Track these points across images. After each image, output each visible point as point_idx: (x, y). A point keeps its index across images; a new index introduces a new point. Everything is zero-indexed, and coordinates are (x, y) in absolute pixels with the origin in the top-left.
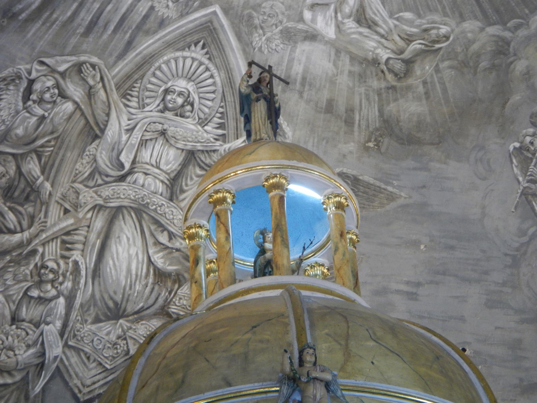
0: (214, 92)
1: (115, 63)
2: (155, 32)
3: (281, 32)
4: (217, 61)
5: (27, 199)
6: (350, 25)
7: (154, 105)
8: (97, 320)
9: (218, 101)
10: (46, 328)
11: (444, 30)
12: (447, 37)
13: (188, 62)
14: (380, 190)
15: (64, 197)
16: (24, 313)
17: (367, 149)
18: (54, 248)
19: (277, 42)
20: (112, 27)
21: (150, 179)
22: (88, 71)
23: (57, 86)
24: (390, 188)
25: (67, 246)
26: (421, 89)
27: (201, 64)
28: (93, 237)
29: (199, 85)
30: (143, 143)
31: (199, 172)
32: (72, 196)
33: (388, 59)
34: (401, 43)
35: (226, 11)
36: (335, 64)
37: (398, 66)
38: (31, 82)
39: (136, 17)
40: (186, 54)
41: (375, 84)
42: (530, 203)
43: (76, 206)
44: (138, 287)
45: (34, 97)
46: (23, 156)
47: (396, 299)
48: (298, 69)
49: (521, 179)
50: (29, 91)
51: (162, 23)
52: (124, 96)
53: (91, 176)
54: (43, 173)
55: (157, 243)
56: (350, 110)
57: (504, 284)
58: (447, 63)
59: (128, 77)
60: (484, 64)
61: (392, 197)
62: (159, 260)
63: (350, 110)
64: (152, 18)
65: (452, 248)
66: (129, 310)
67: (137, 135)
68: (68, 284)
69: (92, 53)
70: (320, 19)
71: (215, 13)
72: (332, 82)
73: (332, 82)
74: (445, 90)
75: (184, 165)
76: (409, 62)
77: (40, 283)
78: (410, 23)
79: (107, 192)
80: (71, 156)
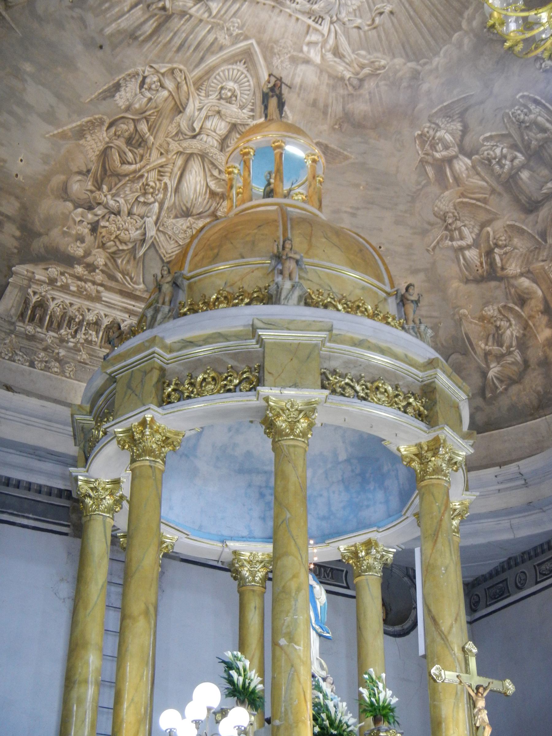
0: (249, 90)
1: (193, 69)
2: (217, 53)
3: (290, 57)
4: (252, 72)
5: (140, 145)
6: (329, 56)
7: (214, 96)
8: (176, 217)
9: (251, 95)
10: (147, 220)
11: (383, 62)
12: (384, 67)
13: (235, 72)
14: (339, 153)
15: (161, 146)
16: (135, 210)
17: (334, 129)
18: (153, 175)
19: (287, 64)
20: (192, 48)
21: (210, 139)
22: (177, 73)
23: (160, 81)
24: (345, 153)
25: (161, 174)
26: (367, 96)
27: (242, 73)
28: (176, 169)
29: (240, 85)
30: (207, 117)
31: (238, 136)
32: (165, 145)
33: (350, 78)
34: (358, 69)
35: (259, 43)
36: (319, 78)
37: (355, 82)
38: (144, 78)
39: (207, 44)
40: (234, 67)
41: (341, 91)
42: (424, 167)
43: (167, 151)
44: (200, 200)
45: (146, 86)
46: (138, 120)
49: (420, 152)
51: (221, 48)
52: (198, 89)
53: (177, 134)
54: (149, 130)
55: (212, 175)
56: (326, 106)
57: (406, 212)
58: (383, 82)
59: (200, 78)
60: (405, 84)
61: (346, 158)
62: (213, 185)
63: (326, 106)
64: (216, 44)
65: (377, 189)
66: (195, 212)
67: (204, 113)
68: (161, 196)
69: (180, 63)
70: (312, 51)
71: (252, 44)
73: (317, 88)
74: (381, 99)
75: (230, 132)
76: (361, 80)
77: (145, 194)
78: (364, 57)
79: (185, 144)
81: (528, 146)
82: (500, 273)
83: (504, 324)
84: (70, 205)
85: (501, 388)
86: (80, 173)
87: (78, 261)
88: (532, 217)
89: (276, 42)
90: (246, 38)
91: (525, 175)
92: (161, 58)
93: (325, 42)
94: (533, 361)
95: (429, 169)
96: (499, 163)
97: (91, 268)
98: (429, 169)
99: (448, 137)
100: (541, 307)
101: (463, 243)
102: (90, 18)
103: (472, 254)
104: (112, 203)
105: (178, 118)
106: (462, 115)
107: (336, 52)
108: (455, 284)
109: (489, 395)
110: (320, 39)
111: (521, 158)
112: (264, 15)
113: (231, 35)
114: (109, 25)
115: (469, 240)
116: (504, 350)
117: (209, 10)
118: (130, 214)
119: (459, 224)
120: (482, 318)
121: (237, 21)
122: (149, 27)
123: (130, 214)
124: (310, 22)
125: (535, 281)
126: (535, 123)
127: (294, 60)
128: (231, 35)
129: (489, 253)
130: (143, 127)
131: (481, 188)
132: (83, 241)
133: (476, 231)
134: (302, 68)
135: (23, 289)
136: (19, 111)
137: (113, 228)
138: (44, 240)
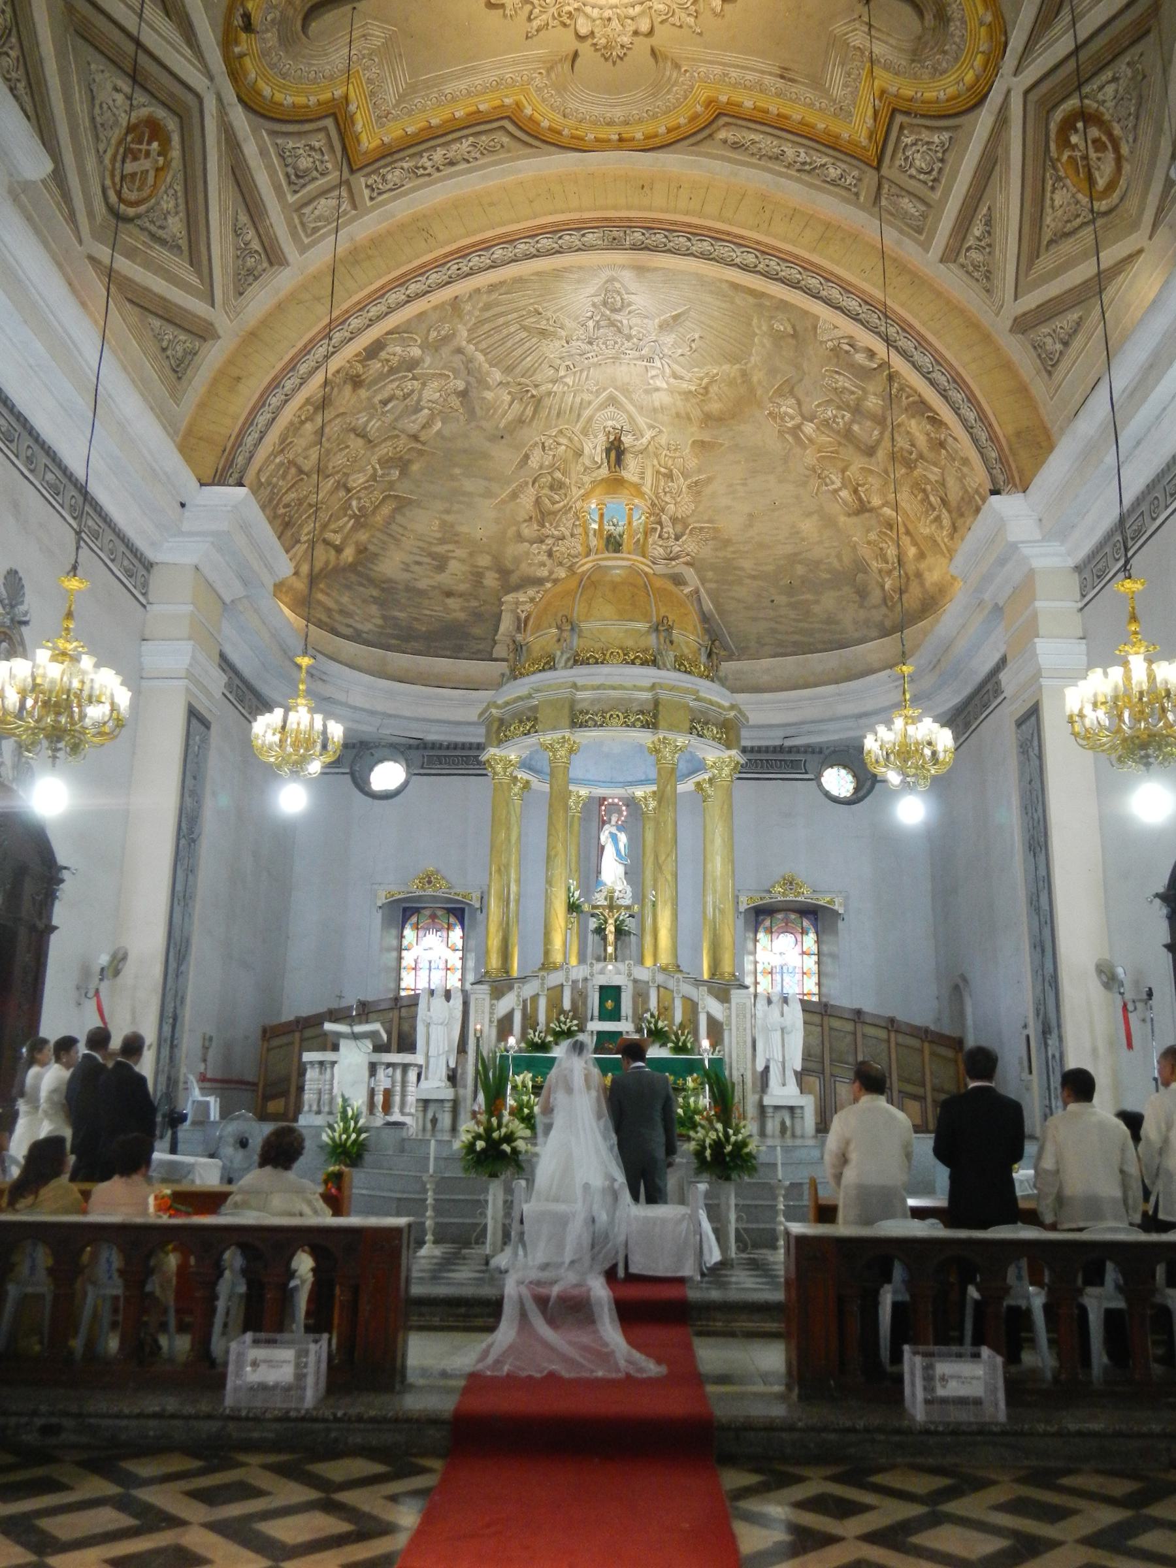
6: (672, 380)
22: (565, 432)
29: (618, 421)
37: (702, 391)
39: (577, 405)
41: (694, 401)
43: (583, 484)
47: (739, 487)
48: (657, 404)
51: (590, 403)
60: (739, 381)
61: (721, 445)
72: (675, 404)
73: (675, 404)
79: (594, 474)
81: (848, 406)
82: (868, 506)
83: (884, 545)
84: (526, 544)
86: (525, 521)
87: (547, 580)
88: (873, 460)
89: (628, 384)
90: (605, 389)
91: (856, 428)
93: (663, 372)
94: (910, 573)
95: (787, 436)
96: (834, 421)
97: (556, 581)
98: (787, 436)
99: (790, 411)
101: (834, 487)
102: (484, 424)
103: (844, 494)
104: (556, 533)
105: (581, 460)
106: (791, 392)
107: (675, 376)
108: (842, 519)
109: (890, 604)
111: (848, 416)
115: (838, 484)
117: (566, 384)
118: (572, 535)
119: (826, 472)
120: (869, 543)
122: (529, 411)
123: (572, 535)
126: (845, 388)
127: (647, 392)
129: (856, 491)
130: (558, 475)
131: (830, 443)
132: (544, 565)
133: (840, 475)
134: (656, 395)
135: (514, 611)
136: (466, 499)
137: (563, 549)
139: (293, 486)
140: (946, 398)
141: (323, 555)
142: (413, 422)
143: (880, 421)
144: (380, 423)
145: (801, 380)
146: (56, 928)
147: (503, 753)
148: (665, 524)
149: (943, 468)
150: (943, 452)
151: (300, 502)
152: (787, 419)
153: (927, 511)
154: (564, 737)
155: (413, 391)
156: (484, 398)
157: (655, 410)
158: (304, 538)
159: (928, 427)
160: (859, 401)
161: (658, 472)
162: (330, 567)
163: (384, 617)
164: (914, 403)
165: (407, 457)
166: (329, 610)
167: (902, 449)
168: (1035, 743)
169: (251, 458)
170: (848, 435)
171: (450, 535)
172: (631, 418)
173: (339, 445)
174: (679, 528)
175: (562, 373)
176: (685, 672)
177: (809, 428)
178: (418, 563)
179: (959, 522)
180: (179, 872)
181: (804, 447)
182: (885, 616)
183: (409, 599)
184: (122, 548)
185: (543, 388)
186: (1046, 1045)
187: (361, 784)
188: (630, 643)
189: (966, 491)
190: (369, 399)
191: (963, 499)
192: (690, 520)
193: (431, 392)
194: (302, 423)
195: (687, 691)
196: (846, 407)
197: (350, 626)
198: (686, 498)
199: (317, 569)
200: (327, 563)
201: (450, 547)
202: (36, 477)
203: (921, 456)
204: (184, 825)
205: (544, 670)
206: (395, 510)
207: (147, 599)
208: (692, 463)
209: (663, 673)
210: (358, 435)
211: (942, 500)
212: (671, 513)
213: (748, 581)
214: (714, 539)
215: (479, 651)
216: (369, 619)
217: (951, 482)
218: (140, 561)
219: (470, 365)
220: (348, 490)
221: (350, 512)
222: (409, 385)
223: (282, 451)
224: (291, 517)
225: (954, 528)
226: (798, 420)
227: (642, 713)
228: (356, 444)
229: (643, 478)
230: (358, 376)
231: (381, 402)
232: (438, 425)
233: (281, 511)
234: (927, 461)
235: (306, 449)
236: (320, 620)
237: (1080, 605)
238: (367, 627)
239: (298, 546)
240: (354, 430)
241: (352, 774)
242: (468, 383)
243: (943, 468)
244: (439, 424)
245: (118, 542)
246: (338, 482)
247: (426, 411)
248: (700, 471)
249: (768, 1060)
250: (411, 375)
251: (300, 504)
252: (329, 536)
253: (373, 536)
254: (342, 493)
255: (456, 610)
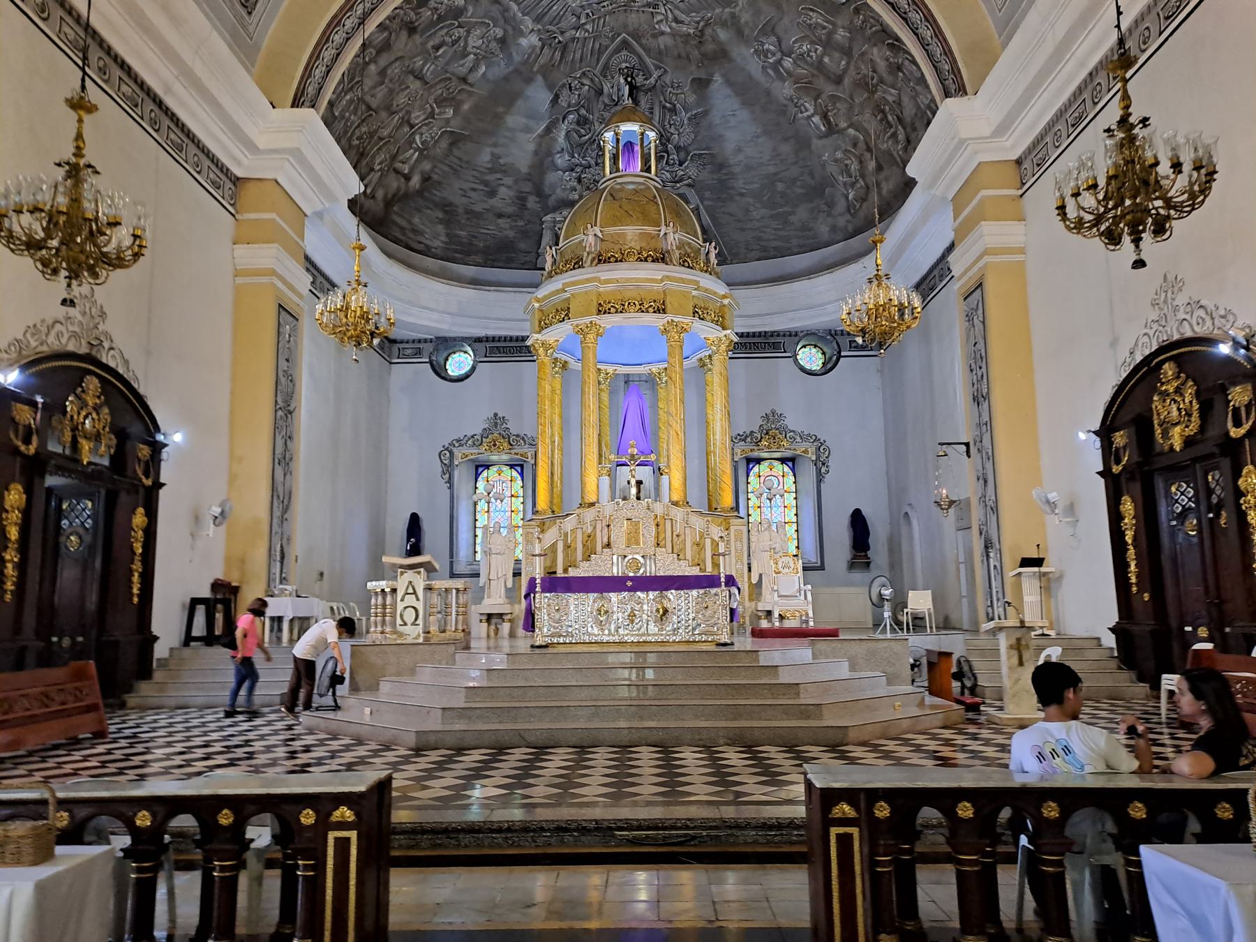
6: (674, 24)
11: (709, 15)
12: (711, 18)
37: (698, 34)
50: (570, 88)
51: (607, 47)
52: (605, 76)
80: (595, 103)
83: (848, 162)
85: (858, 206)
86: (558, 152)
88: (841, 88)
90: (619, 35)
91: (826, 60)
92: (573, 70)
93: (667, 18)
95: (770, 71)
96: (808, 55)
99: (772, 48)
100: (865, 147)
103: (816, 119)
106: (773, 31)
107: (676, 20)
110: (662, 17)
111: (820, 49)
112: (622, 17)
113: (608, 38)
114: (533, 66)
115: (812, 111)
116: (853, 179)
117: (587, 31)
118: (597, 164)
119: (801, 101)
120: (836, 161)
121: (607, 29)
122: (558, 55)
123: (597, 164)
124: (651, 10)
125: (857, 130)
126: (817, 23)
128: (608, 38)
130: (583, 112)
134: (661, 40)
136: (507, 134)
137: (589, 176)
138: (553, 197)
139: (363, 121)
140: (905, 19)
141: (394, 183)
142: (462, 66)
143: (847, 52)
144: (433, 66)
145: (781, 19)
146: (164, 485)
147: (543, 338)
148: (670, 151)
149: (899, 90)
150: (900, 74)
151: (371, 135)
152: (769, 55)
153: (885, 130)
154: (591, 322)
155: (460, 38)
156: (520, 44)
157: (660, 52)
158: (377, 168)
159: (888, 53)
160: (831, 34)
161: (664, 107)
162: (402, 192)
163: (448, 235)
164: (876, 32)
165: (459, 98)
166: (402, 229)
167: (865, 76)
168: (980, 312)
169: (321, 89)
170: (820, 66)
171: (497, 167)
172: (640, 58)
173: (400, 85)
174: (682, 154)
175: (583, 21)
176: (689, 267)
177: (788, 63)
178: (474, 190)
179: (913, 136)
180: (279, 438)
181: (783, 80)
182: (848, 221)
183: (468, 219)
184: (207, 163)
185: (567, 34)
186: (988, 556)
187: (440, 371)
188: (644, 245)
189: (919, 107)
190: (423, 44)
191: (916, 114)
192: (690, 148)
193: (474, 41)
194: (367, 64)
195: (690, 282)
196: (820, 42)
197: (420, 242)
198: (687, 129)
199: (389, 196)
200: (399, 189)
201: (499, 176)
202: (111, 88)
203: (881, 81)
204: (279, 401)
205: (574, 268)
206: (452, 144)
207: (235, 209)
208: (692, 98)
209: (671, 267)
210: (416, 77)
211: (898, 117)
212: (675, 142)
213: (738, 198)
214: (711, 163)
215: (525, 263)
216: (436, 236)
217: (906, 101)
218: (226, 175)
219: (506, 14)
220: (412, 127)
221: (414, 145)
222: (457, 33)
223: (351, 89)
224: (364, 148)
225: (908, 141)
226: (779, 55)
227: (655, 301)
228: (415, 85)
229: (652, 113)
230: (412, 23)
231: (433, 47)
232: (483, 68)
233: (356, 142)
234: (886, 85)
235: (374, 87)
236: (395, 237)
237: (1020, 192)
238: (436, 243)
239: (373, 173)
240: (412, 72)
241: (431, 363)
242: (505, 31)
243: (899, 90)
244: (483, 68)
245: (202, 157)
246: (403, 118)
247: (472, 56)
248: (698, 105)
249: (761, 575)
250: (457, 24)
251: (372, 137)
252: (398, 165)
253: (435, 167)
254: (406, 129)
255: (505, 229)
